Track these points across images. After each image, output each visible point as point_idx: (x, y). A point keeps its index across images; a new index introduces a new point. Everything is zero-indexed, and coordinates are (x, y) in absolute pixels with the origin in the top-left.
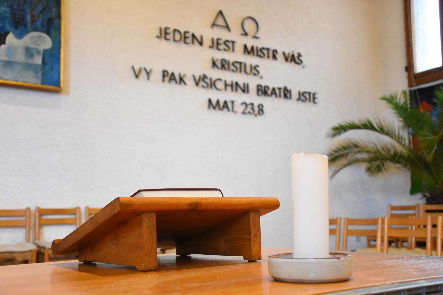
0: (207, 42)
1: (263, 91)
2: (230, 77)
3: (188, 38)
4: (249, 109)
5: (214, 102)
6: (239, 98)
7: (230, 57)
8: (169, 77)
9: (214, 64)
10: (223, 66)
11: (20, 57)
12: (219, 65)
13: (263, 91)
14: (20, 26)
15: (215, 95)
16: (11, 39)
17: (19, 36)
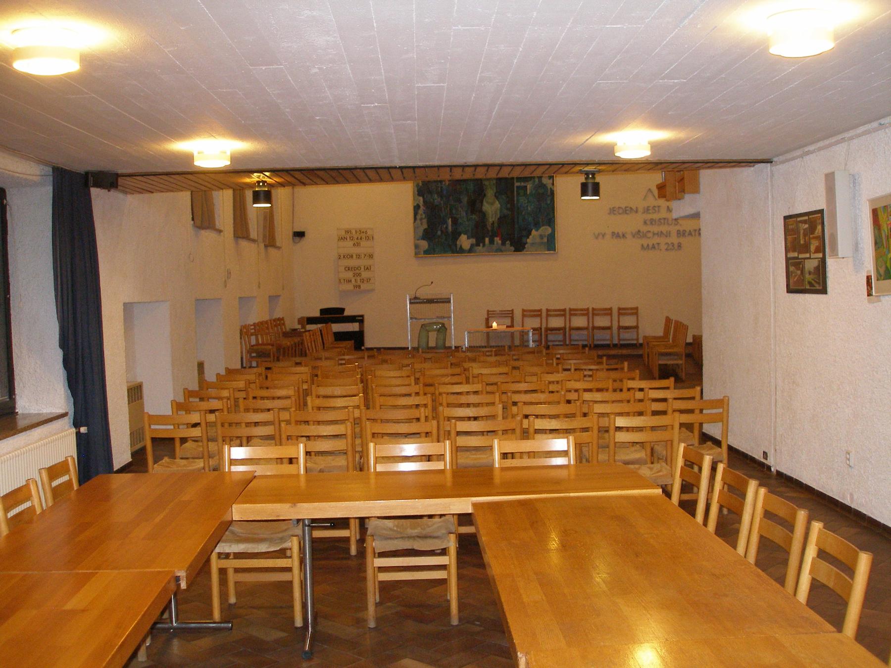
0: (640, 210)
1: (680, 234)
2: (655, 229)
3: (627, 210)
4: (671, 247)
5: (645, 246)
6: (662, 241)
7: (655, 216)
8: (616, 235)
9: (645, 223)
10: (651, 223)
11: (538, 240)
12: (648, 222)
13: (680, 234)
14: (537, 225)
15: (645, 242)
16: (534, 232)
17: (537, 230)
